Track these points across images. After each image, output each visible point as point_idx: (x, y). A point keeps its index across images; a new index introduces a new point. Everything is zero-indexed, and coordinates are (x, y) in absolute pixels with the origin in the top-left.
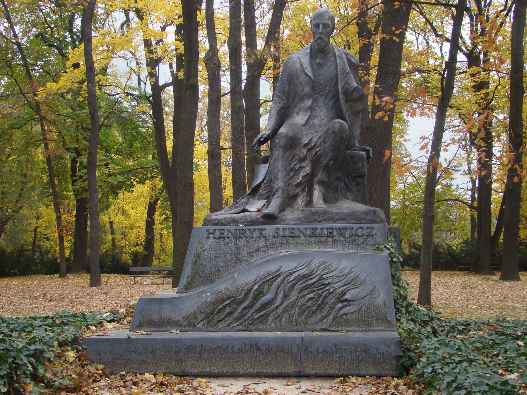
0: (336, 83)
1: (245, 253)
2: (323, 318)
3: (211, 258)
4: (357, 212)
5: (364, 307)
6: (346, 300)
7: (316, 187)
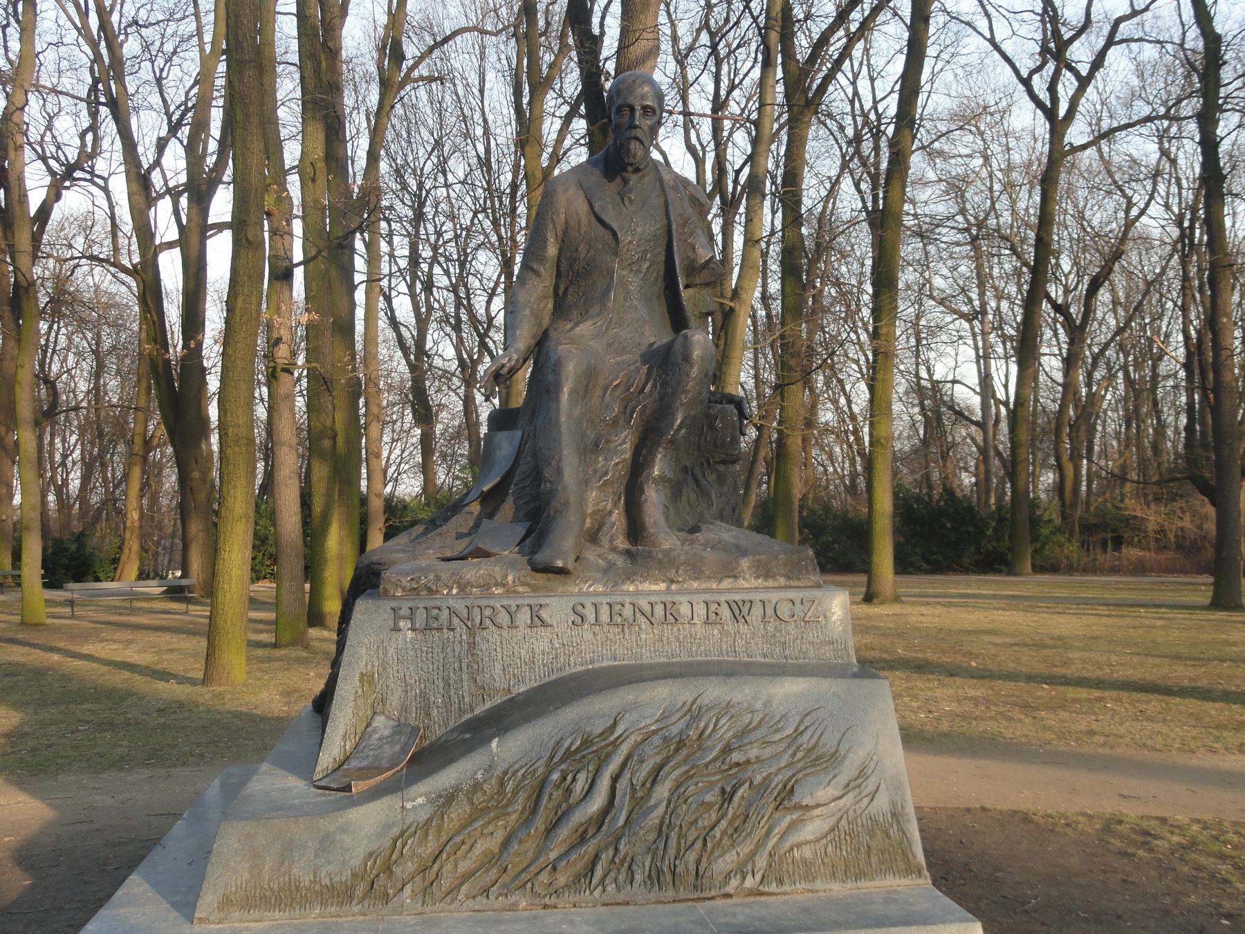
5: (844, 823)
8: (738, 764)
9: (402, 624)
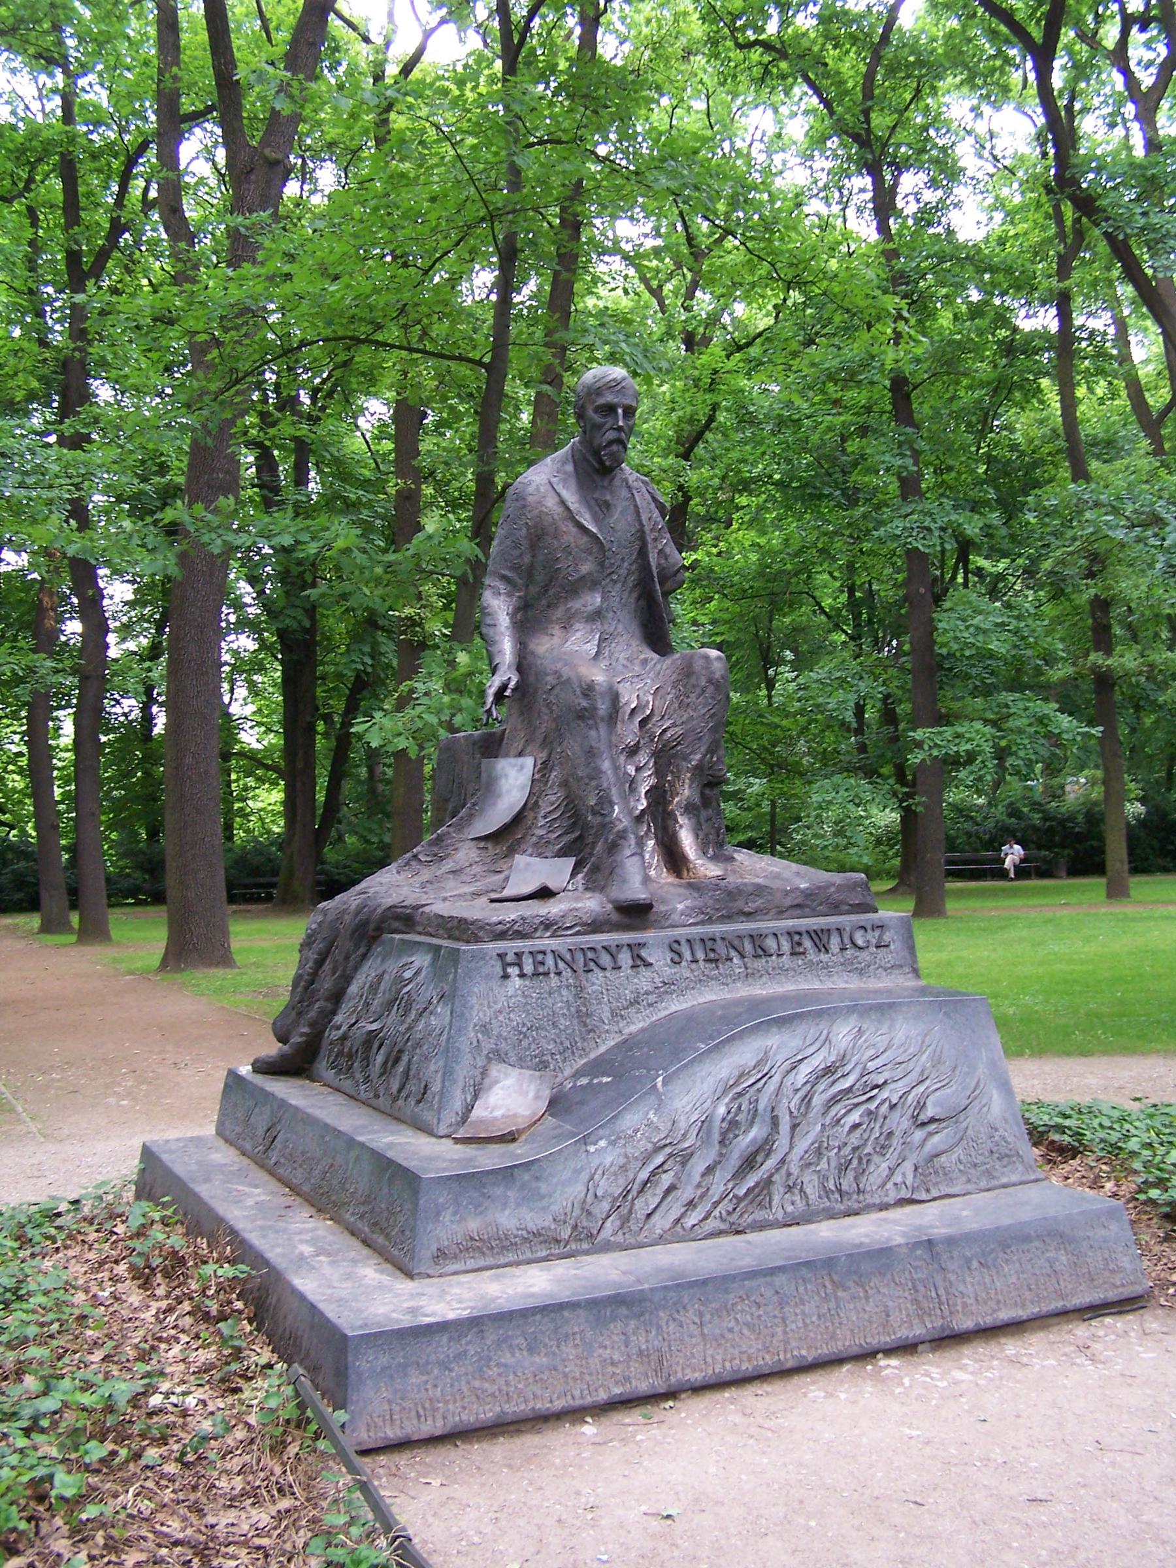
0: (643, 553)
1: (606, 1015)
2: (892, 1171)
3: (521, 1033)
4: (827, 887)
5: (970, 1132)
6: (932, 1120)
7: (681, 820)
8: (877, 1086)
9: (510, 970)
